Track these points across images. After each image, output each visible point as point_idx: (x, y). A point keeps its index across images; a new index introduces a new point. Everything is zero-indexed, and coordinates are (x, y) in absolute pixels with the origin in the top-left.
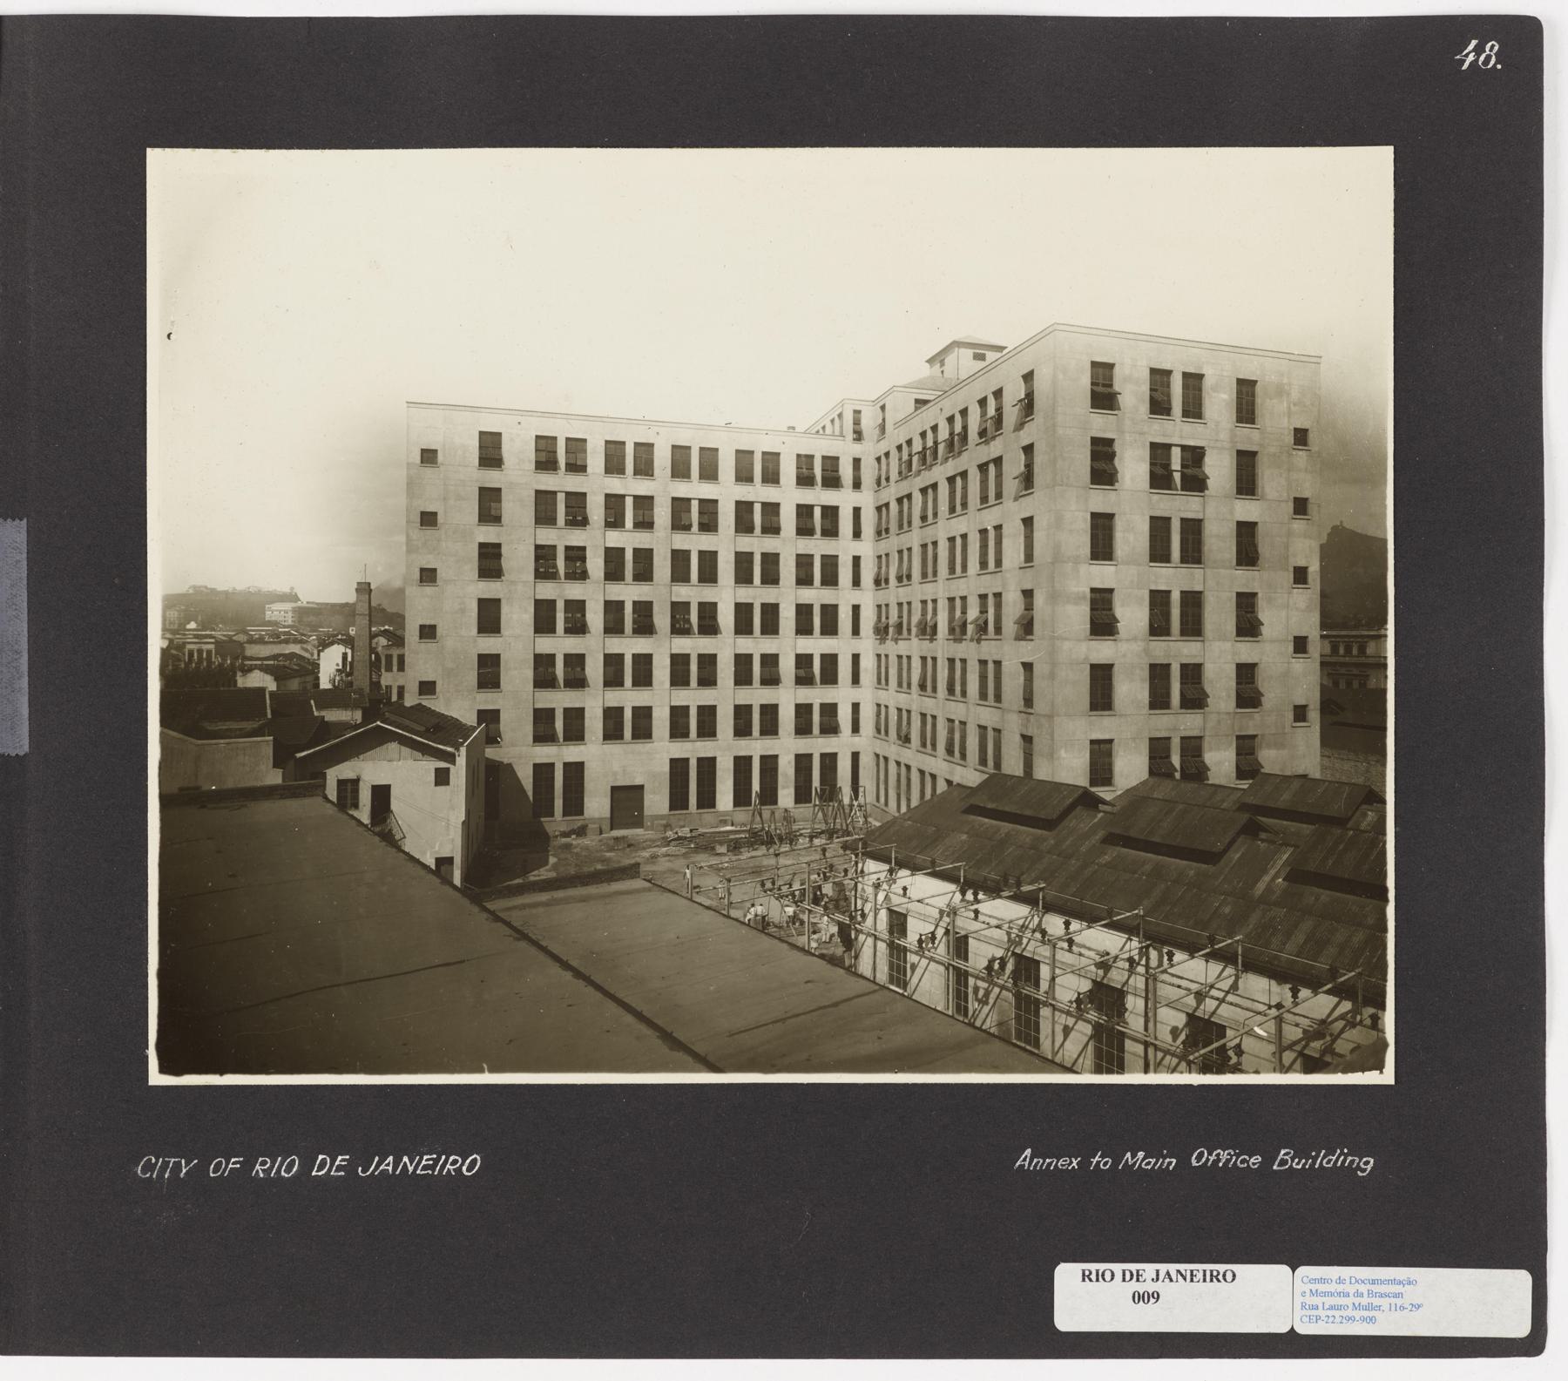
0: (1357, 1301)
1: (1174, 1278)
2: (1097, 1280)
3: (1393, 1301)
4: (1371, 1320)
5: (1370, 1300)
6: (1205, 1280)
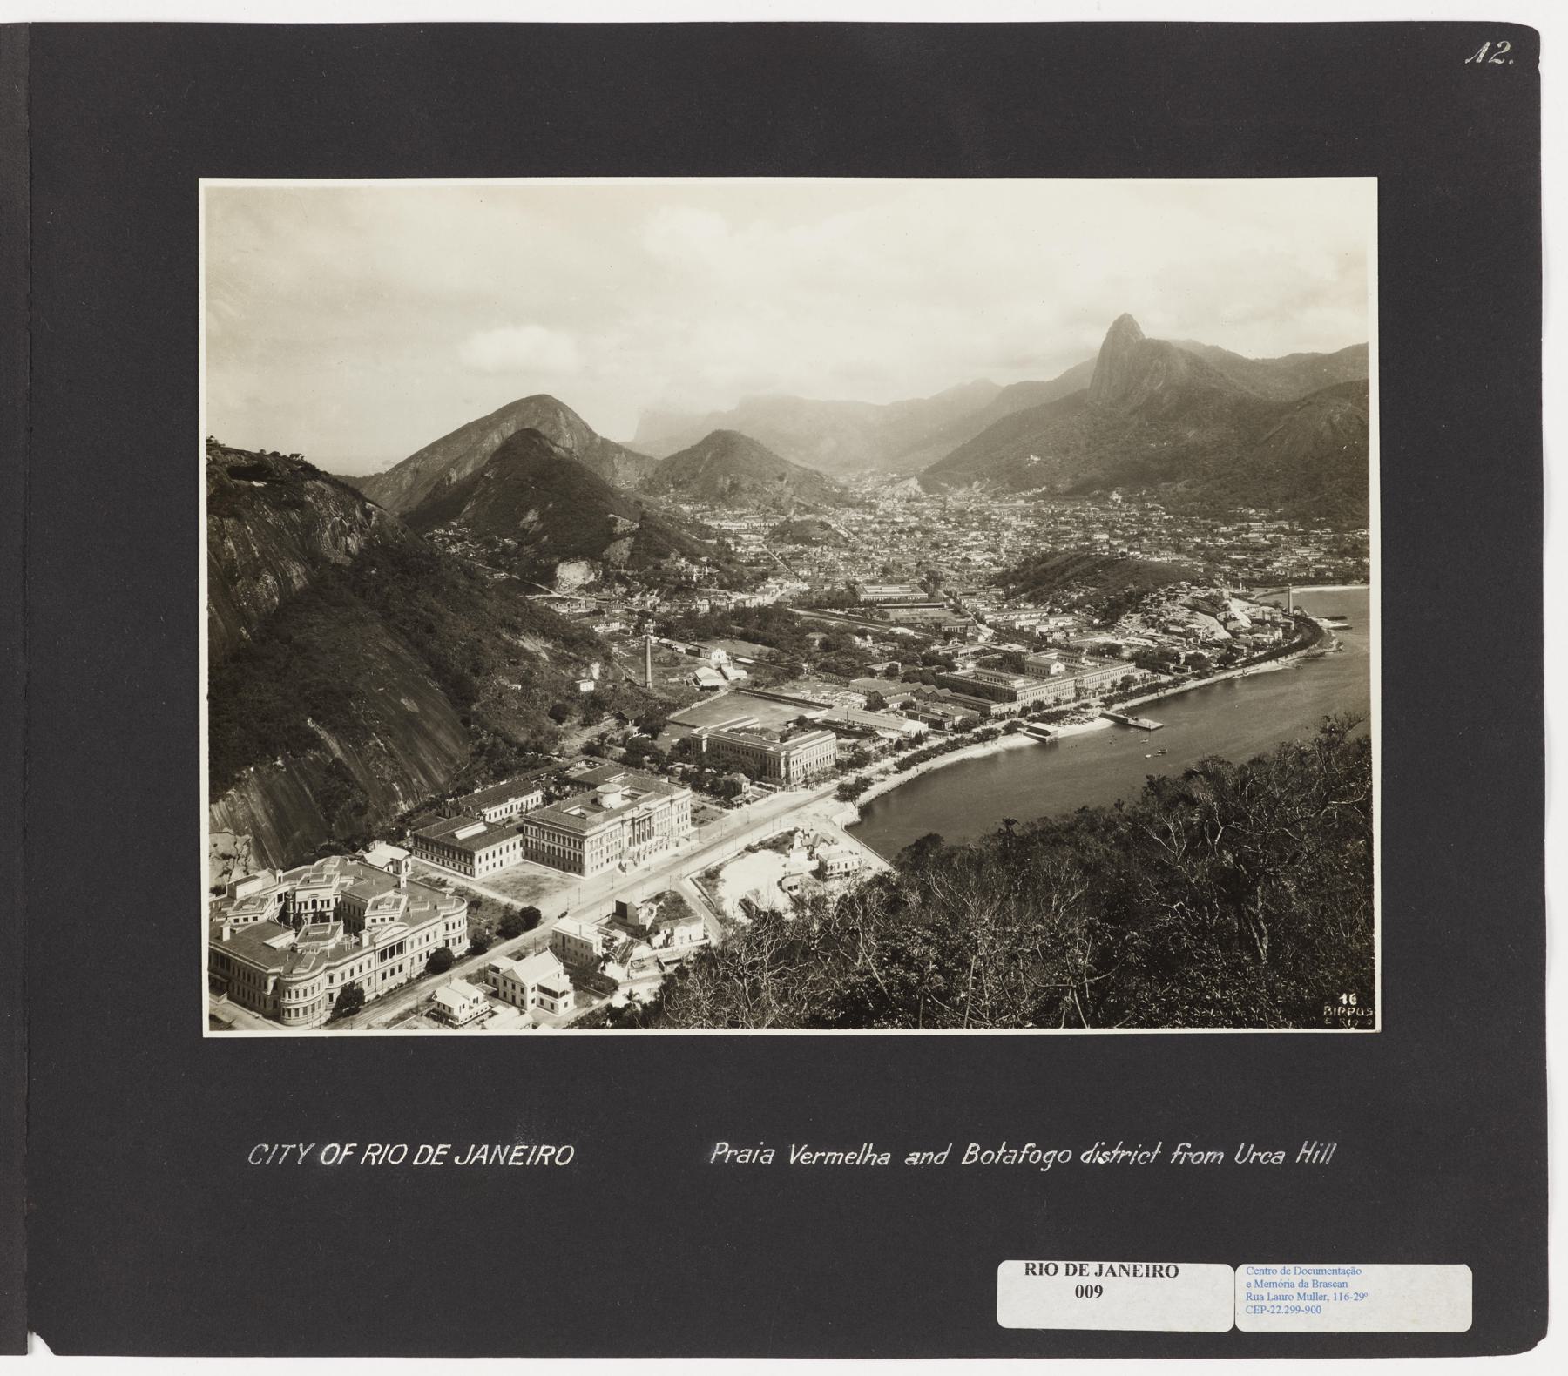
0: (1302, 1291)
1: (1117, 1274)
2: (1041, 1273)
3: (1338, 1290)
4: (1316, 1310)
5: (1316, 1290)
6: (1147, 1275)
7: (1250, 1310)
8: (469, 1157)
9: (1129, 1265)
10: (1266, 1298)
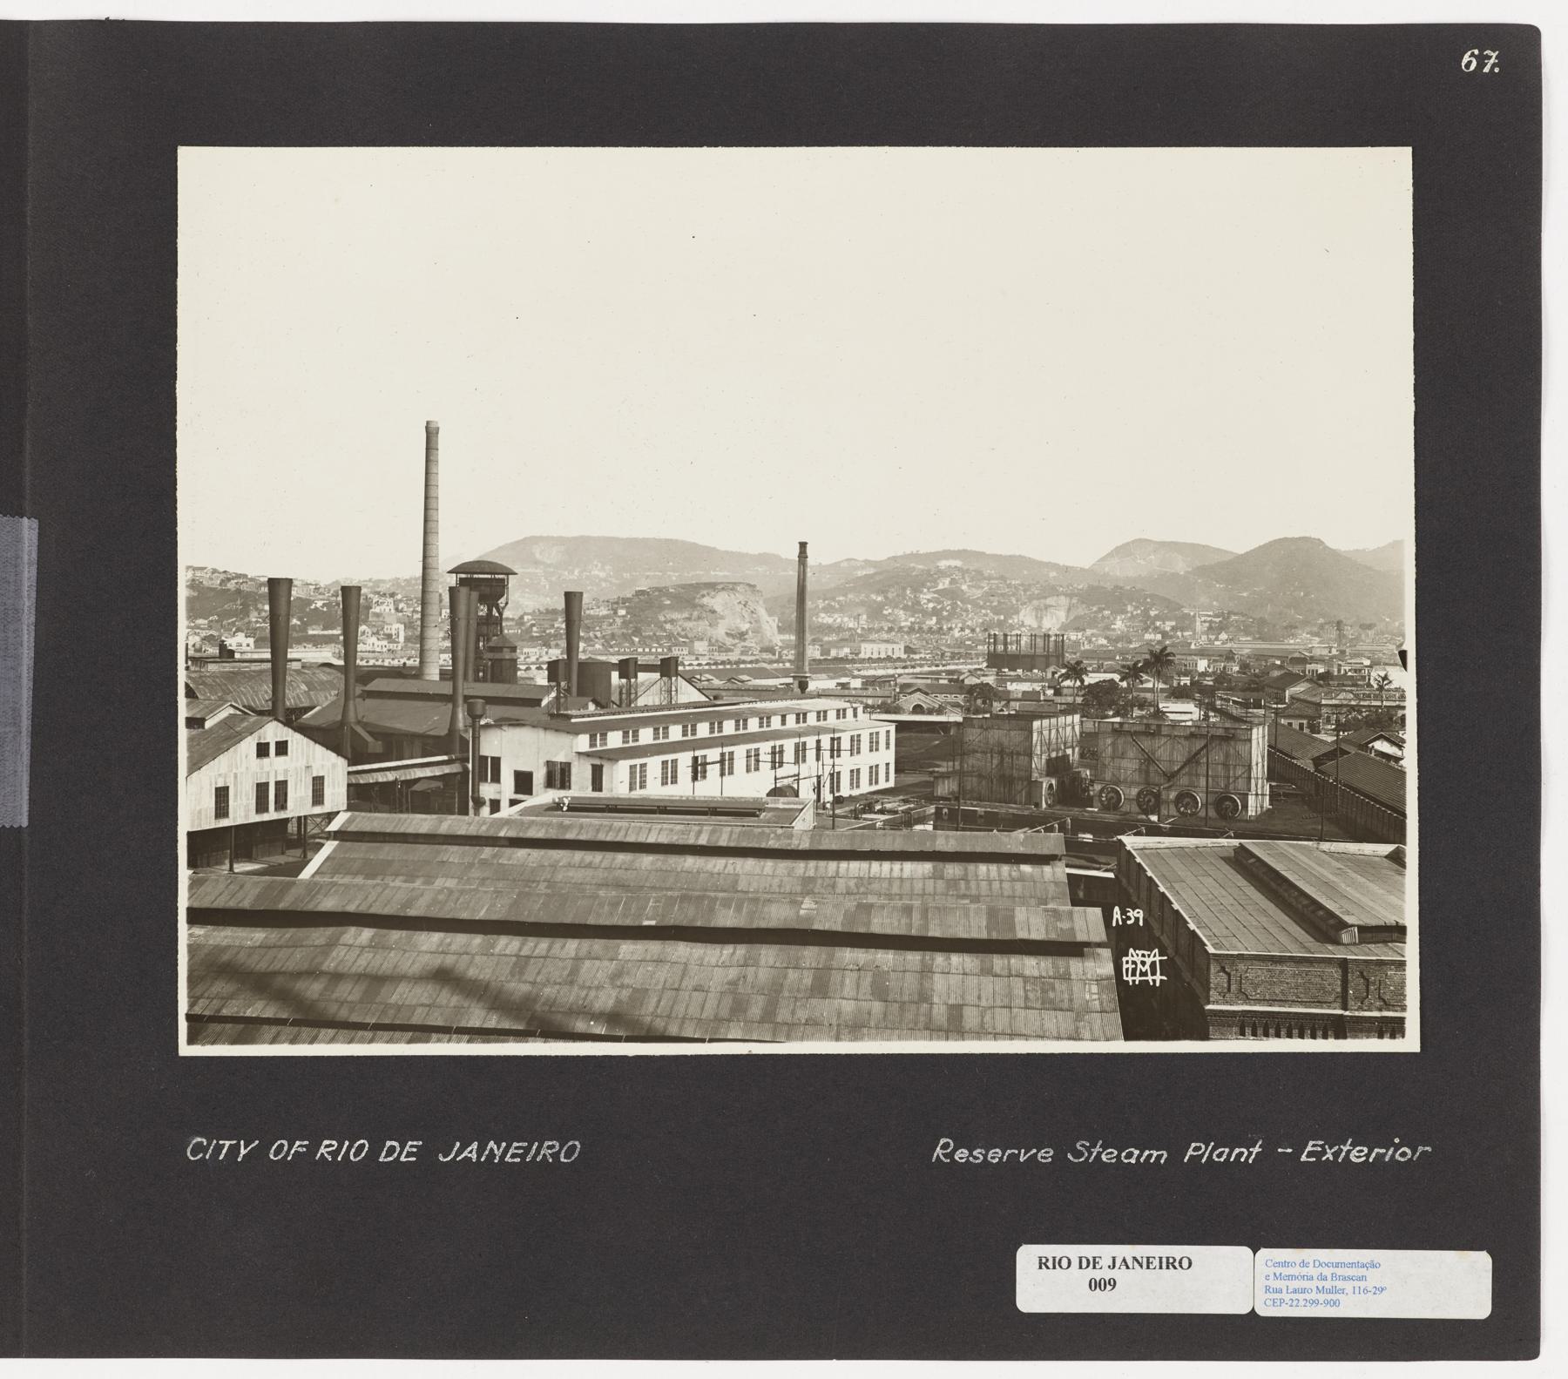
1: (1131, 1266)
2: (1054, 1268)
3: (1357, 1284)
4: (1335, 1303)
5: (1334, 1283)
6: (1161, 1268)
7: (1268, 1302)
10: (1284, 1290)
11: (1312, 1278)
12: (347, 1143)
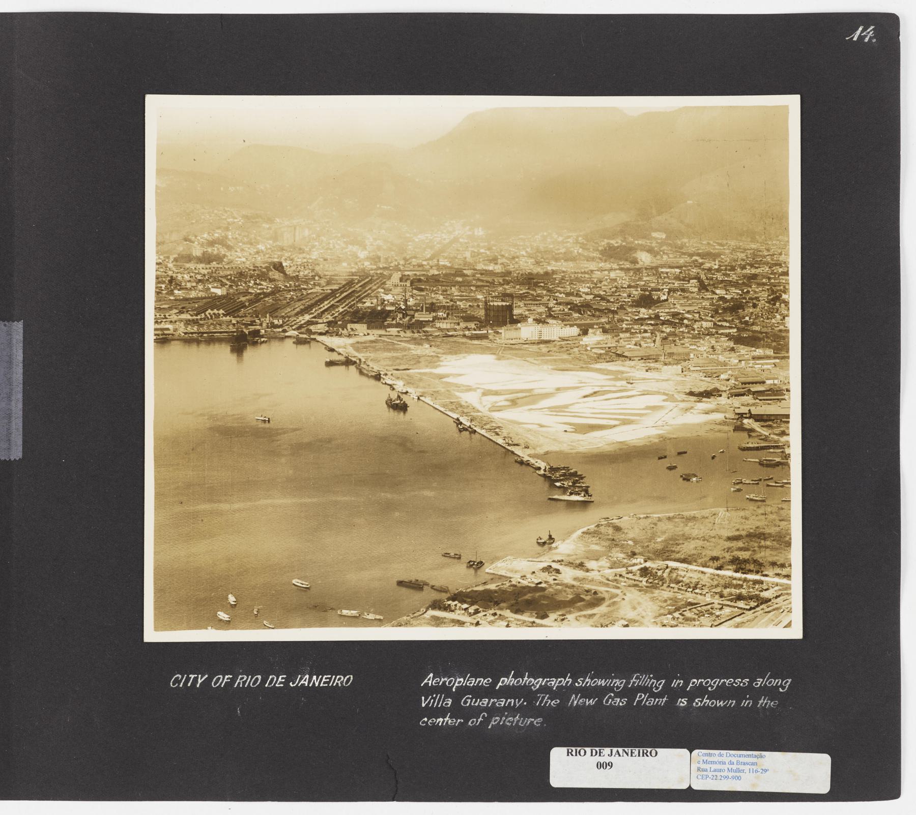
1: (621, 755)
2: (576, 755)
5: (738, 767)
6: (639, 756)
8: (297, 682)
9: (628, 750)
10: (709, 770)
11: (725, 763)
12: (250, 677)
